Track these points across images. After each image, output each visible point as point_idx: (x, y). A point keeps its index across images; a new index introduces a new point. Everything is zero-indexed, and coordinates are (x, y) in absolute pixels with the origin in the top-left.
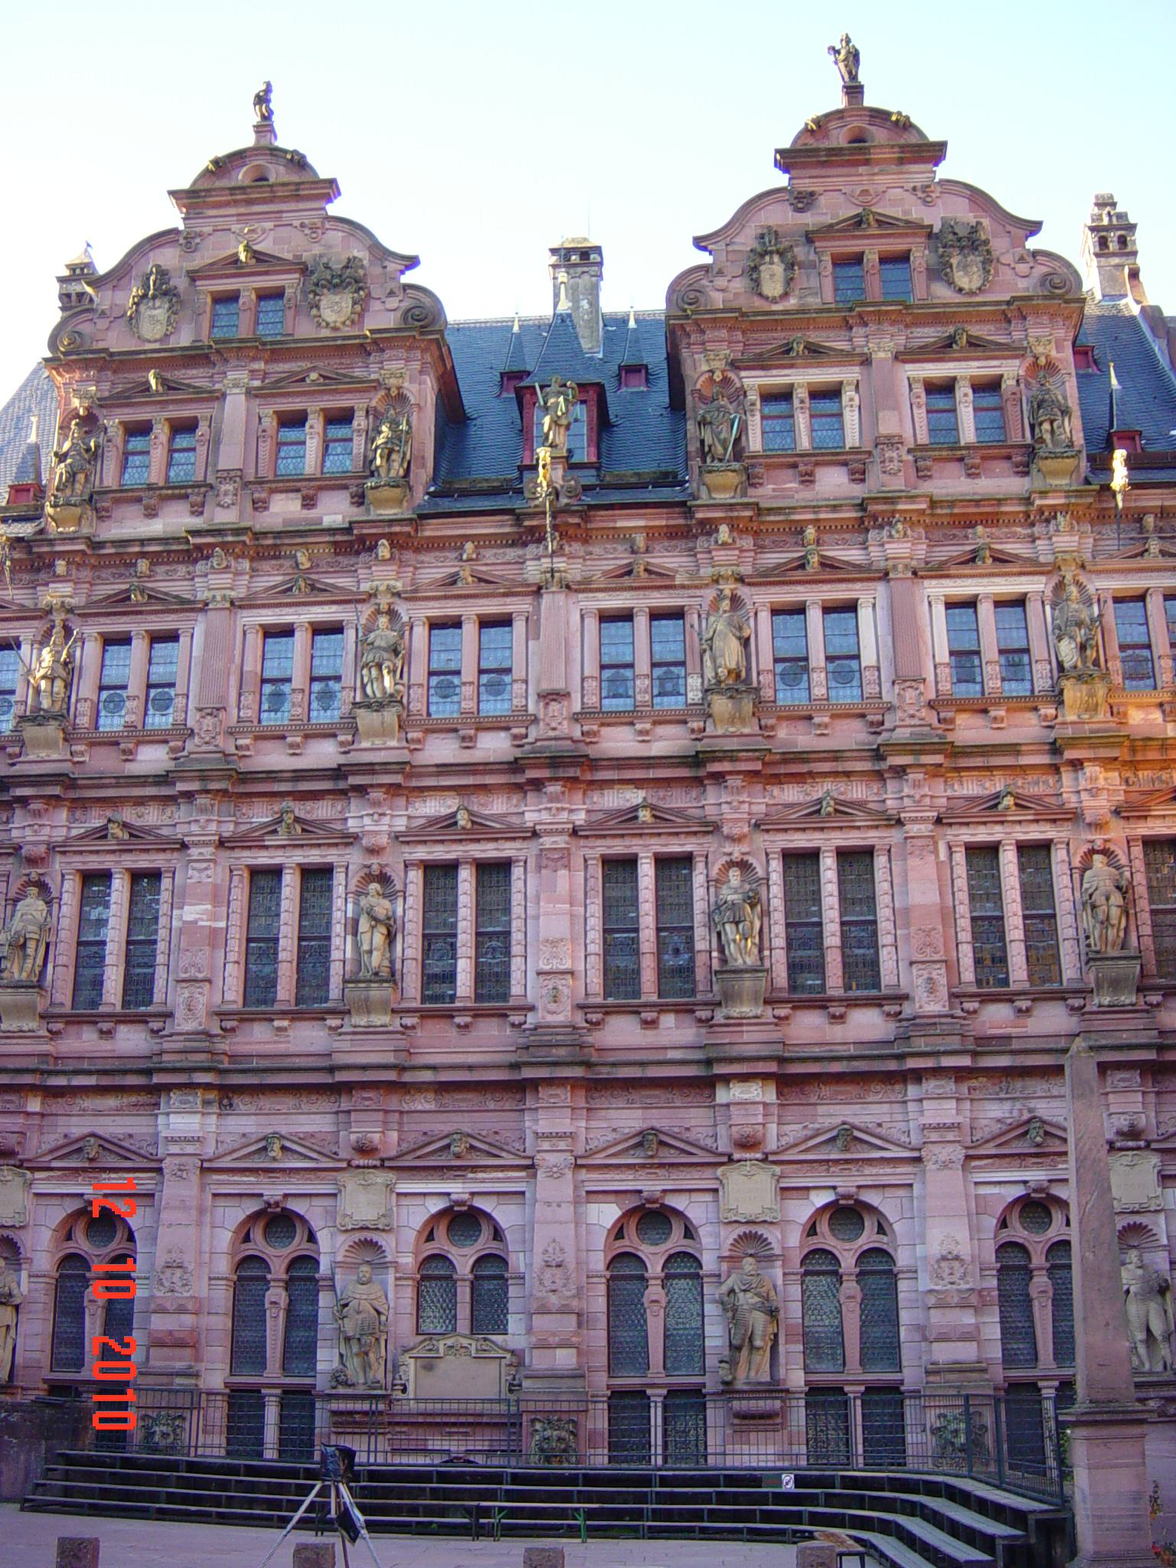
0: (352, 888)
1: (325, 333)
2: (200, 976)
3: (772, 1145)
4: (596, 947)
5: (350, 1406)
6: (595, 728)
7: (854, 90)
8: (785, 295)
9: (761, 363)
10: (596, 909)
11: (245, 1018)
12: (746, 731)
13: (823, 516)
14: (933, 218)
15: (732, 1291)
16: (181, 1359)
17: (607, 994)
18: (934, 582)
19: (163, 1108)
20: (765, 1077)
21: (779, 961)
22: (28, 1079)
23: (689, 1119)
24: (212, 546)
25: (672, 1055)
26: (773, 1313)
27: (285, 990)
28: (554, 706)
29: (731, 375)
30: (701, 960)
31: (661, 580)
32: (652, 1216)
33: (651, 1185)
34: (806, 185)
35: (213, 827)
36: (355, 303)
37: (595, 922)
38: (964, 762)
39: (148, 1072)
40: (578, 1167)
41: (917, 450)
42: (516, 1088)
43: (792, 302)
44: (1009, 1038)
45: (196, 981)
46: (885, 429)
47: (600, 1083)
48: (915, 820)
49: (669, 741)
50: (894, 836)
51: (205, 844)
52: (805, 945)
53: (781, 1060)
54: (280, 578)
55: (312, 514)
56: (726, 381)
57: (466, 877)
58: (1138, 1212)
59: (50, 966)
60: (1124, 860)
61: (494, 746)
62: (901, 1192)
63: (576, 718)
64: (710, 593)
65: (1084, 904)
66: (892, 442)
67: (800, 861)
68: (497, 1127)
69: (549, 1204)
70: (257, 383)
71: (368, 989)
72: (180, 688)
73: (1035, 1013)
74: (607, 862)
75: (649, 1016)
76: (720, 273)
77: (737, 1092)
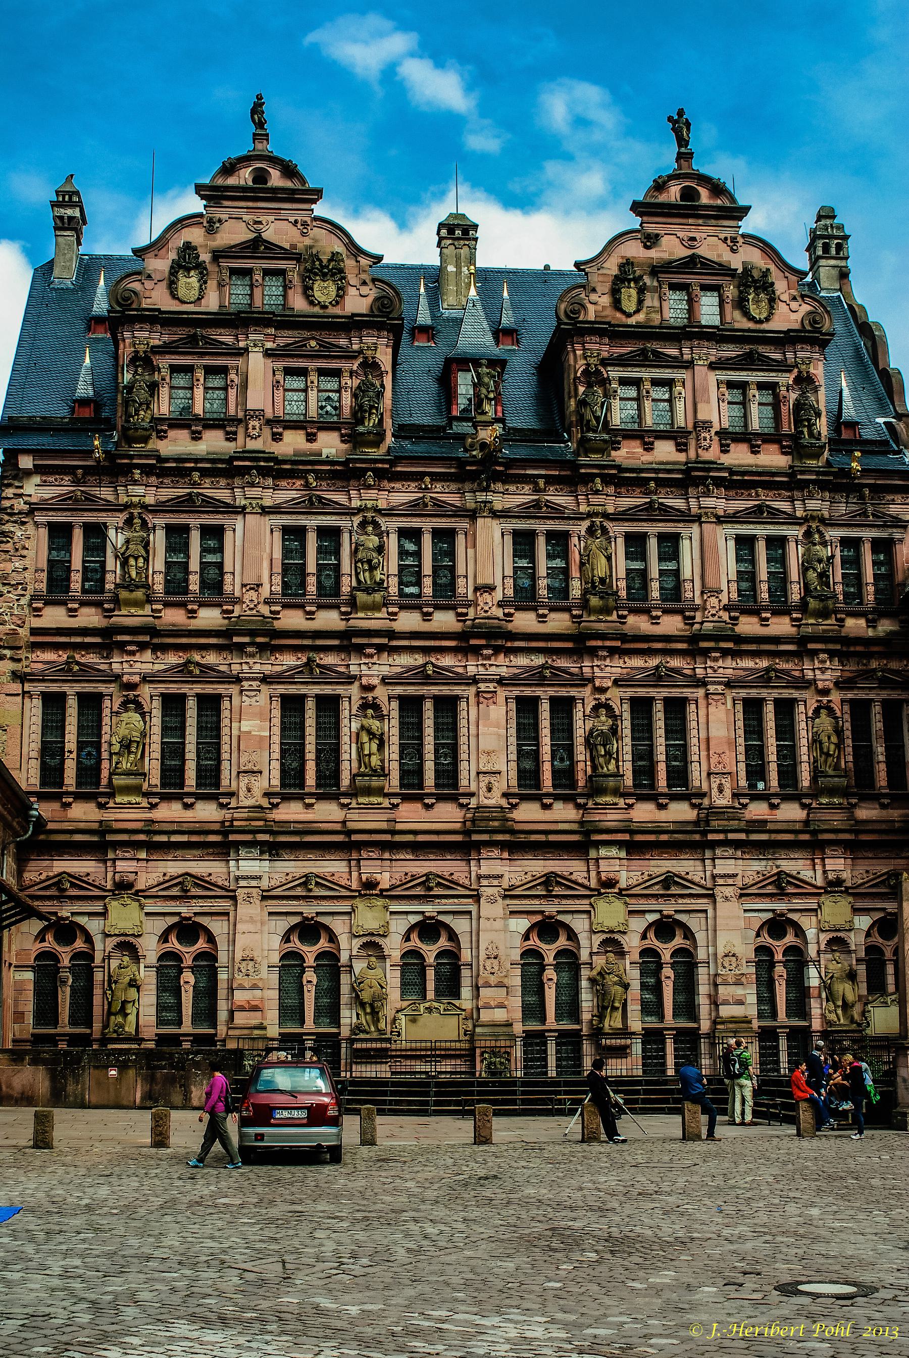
0: (354, 712)
1: (317, 310)
2: (255, 769)
3: (623, 884)
4: (514, 757)
5: (369, 1045)
6: (512, 611)
7: (684, 157)
8: (637, 311)
9: (621, 361)
10: (513, 731)
11: (286, 798)
12: (609, 618)
13: (661, 475)
14: (736, 262)
15: (600, 973)
16: (255, 1018)
17: (519, 786)
18: (729, 526)
19: (233, 855)
20: (619, 844)
21: (627, 768)
22: (142, 837)
23: (573, 868)
24: (250, 468)
25: (561, 827)
26: (626, 986)
27: (311, 779)
28: (486, 595)
29: (600, 368)
30: (581, 766)
31: (557, 513)
32: (547, 928)
33: (551, 908)
34: (651, 228)
35: (257, 667)
36: (339, 289)
37: (513, 740)
38: (745, 647)
39: (225, 833)
40: (505, 897)
41: (722, 434)
42: (465, 846)
43: (641, 317)
44: (765, 822)
45: (254, 772)
46: (701, 416)
47: (519, 845)
48: (714, 683)
49: (559, 622)
50: (701, 692)
51: (254, 679)
52: (641, 758)
53: (632, 832)
54: (294, 494)
55: (314, 446)
56: (598, 372)
57: (428, 705)
58: (839, 930)
59: (147, 759)
60: (839, 714)
61: (444, 620)
62: (700, 915)
63: (500, 605)
64: (586, 524)
65: (814, 741)
66: (707, 425)
67: (641, 707)
68: (452, 870)
69: (488, 919)
70: (269, 345)
71: (370, 780)
72: (228, 567)
73: (782, 806)
74: (519, 700)
75: (547, 801)
76: (594, 290)
77: (603, 852)
